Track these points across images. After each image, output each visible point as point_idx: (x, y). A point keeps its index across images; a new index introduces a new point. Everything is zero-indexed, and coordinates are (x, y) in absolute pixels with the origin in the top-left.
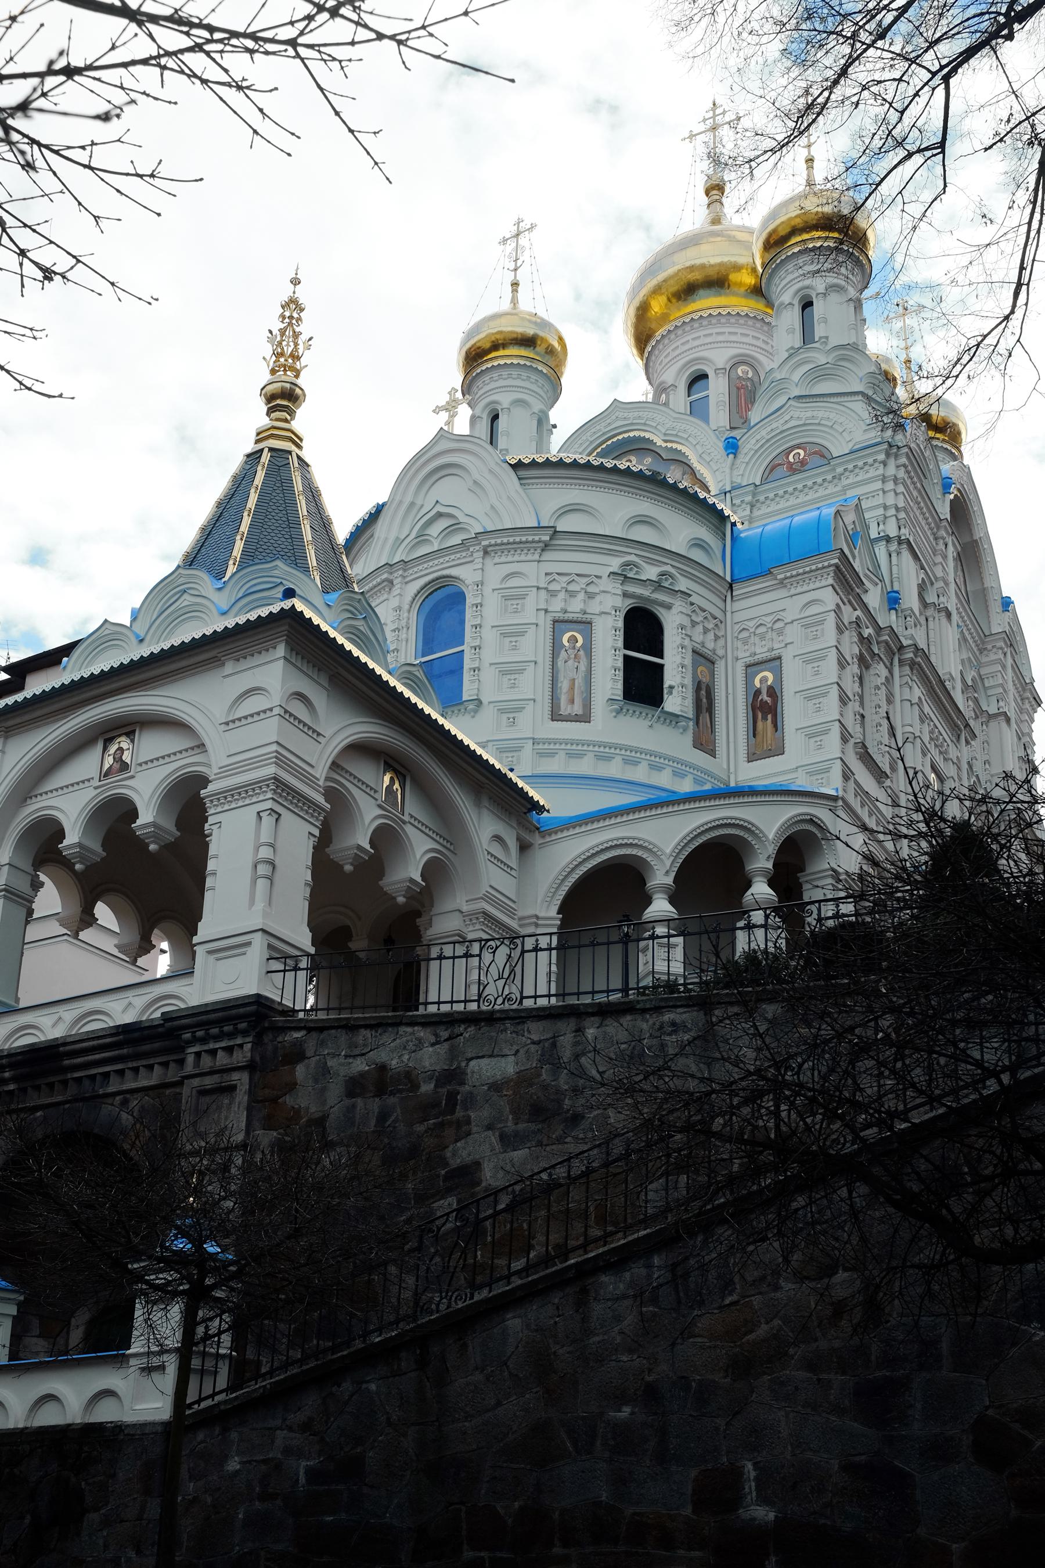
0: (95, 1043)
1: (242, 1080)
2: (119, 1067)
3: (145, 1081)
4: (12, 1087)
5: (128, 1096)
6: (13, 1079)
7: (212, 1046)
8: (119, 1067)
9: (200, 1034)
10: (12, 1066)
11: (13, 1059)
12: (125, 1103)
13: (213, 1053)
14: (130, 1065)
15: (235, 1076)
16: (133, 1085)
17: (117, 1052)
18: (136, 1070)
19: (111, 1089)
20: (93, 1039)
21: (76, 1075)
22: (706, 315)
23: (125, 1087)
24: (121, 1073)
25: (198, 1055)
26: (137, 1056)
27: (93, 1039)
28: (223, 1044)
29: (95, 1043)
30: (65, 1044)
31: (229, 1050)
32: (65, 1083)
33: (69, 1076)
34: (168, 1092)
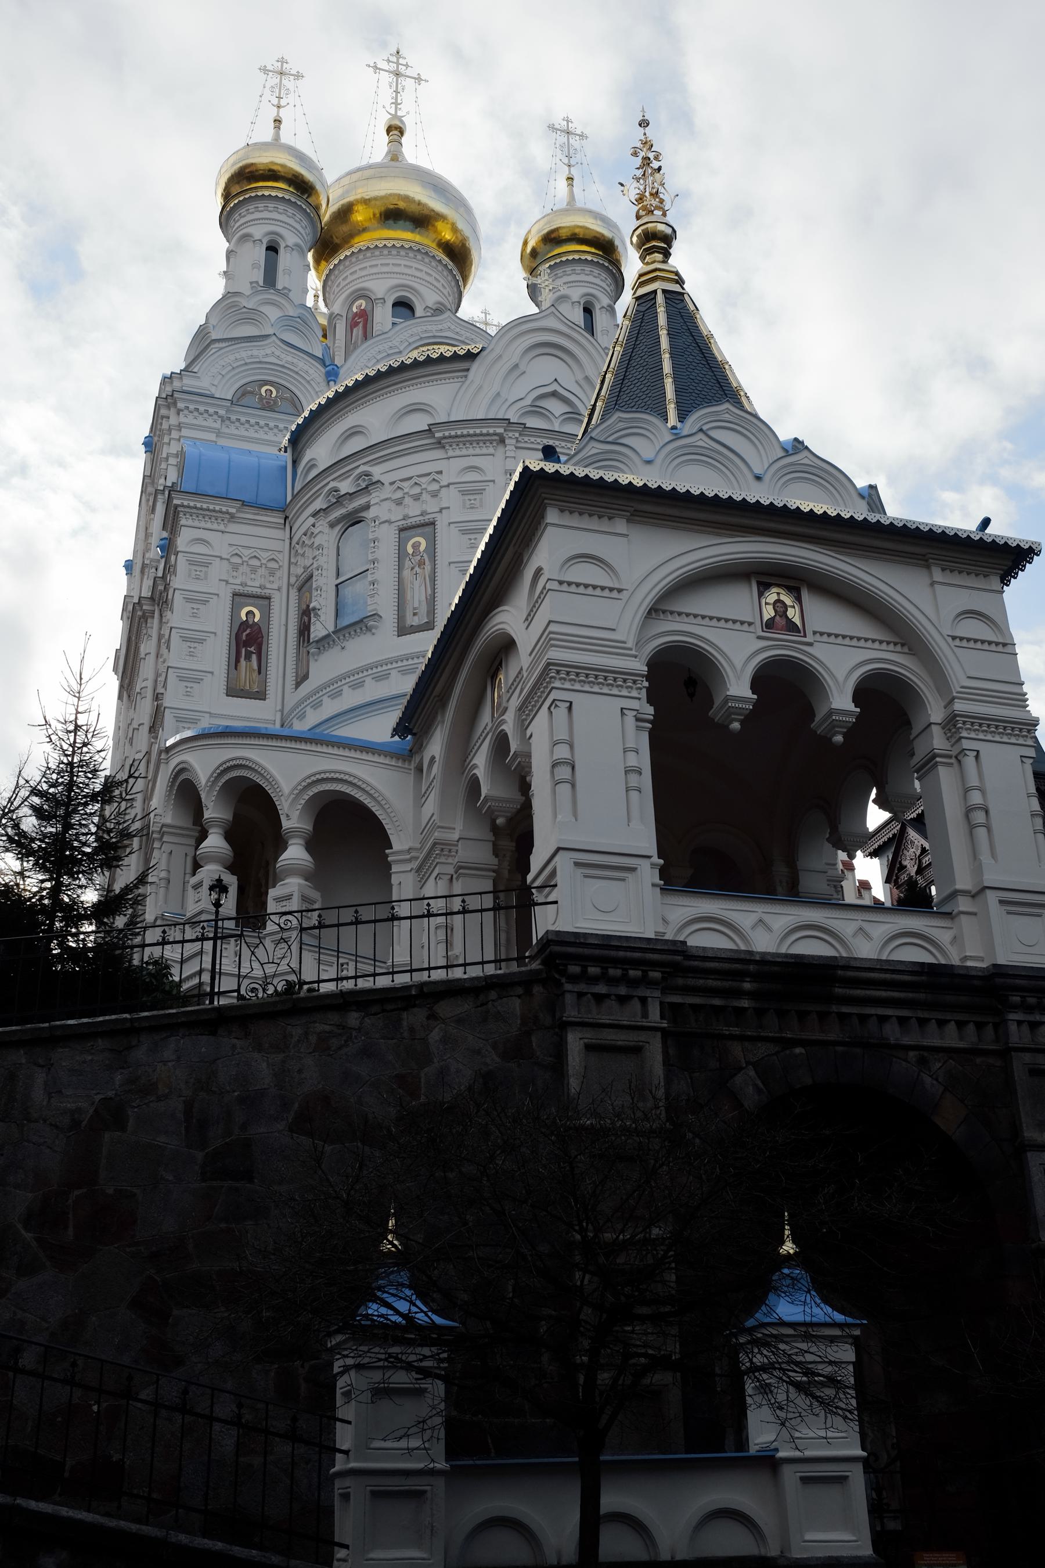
0: (888, 976)
3: (951, 1037)
4: (745, 1003)
5: (926, 1054)
6: (751, 995)
9: (1032, 1000)
12: (922, 1062)
14: (921, 1014)
16: (937, 1042)
17: (910, 995)
18: (922, 1022)
19: (906, 1041)
20: (881, 970)
21: (845, 1009)
22: (407, 246)
23: (926, 1042)
24: (902, 1021)
25: (1019, 1023)
27: (881, 970)
29: (888, 976)
30: (847, 967)
32: (823, 1016)
33: (834, 1008)
34: (978, 1060)
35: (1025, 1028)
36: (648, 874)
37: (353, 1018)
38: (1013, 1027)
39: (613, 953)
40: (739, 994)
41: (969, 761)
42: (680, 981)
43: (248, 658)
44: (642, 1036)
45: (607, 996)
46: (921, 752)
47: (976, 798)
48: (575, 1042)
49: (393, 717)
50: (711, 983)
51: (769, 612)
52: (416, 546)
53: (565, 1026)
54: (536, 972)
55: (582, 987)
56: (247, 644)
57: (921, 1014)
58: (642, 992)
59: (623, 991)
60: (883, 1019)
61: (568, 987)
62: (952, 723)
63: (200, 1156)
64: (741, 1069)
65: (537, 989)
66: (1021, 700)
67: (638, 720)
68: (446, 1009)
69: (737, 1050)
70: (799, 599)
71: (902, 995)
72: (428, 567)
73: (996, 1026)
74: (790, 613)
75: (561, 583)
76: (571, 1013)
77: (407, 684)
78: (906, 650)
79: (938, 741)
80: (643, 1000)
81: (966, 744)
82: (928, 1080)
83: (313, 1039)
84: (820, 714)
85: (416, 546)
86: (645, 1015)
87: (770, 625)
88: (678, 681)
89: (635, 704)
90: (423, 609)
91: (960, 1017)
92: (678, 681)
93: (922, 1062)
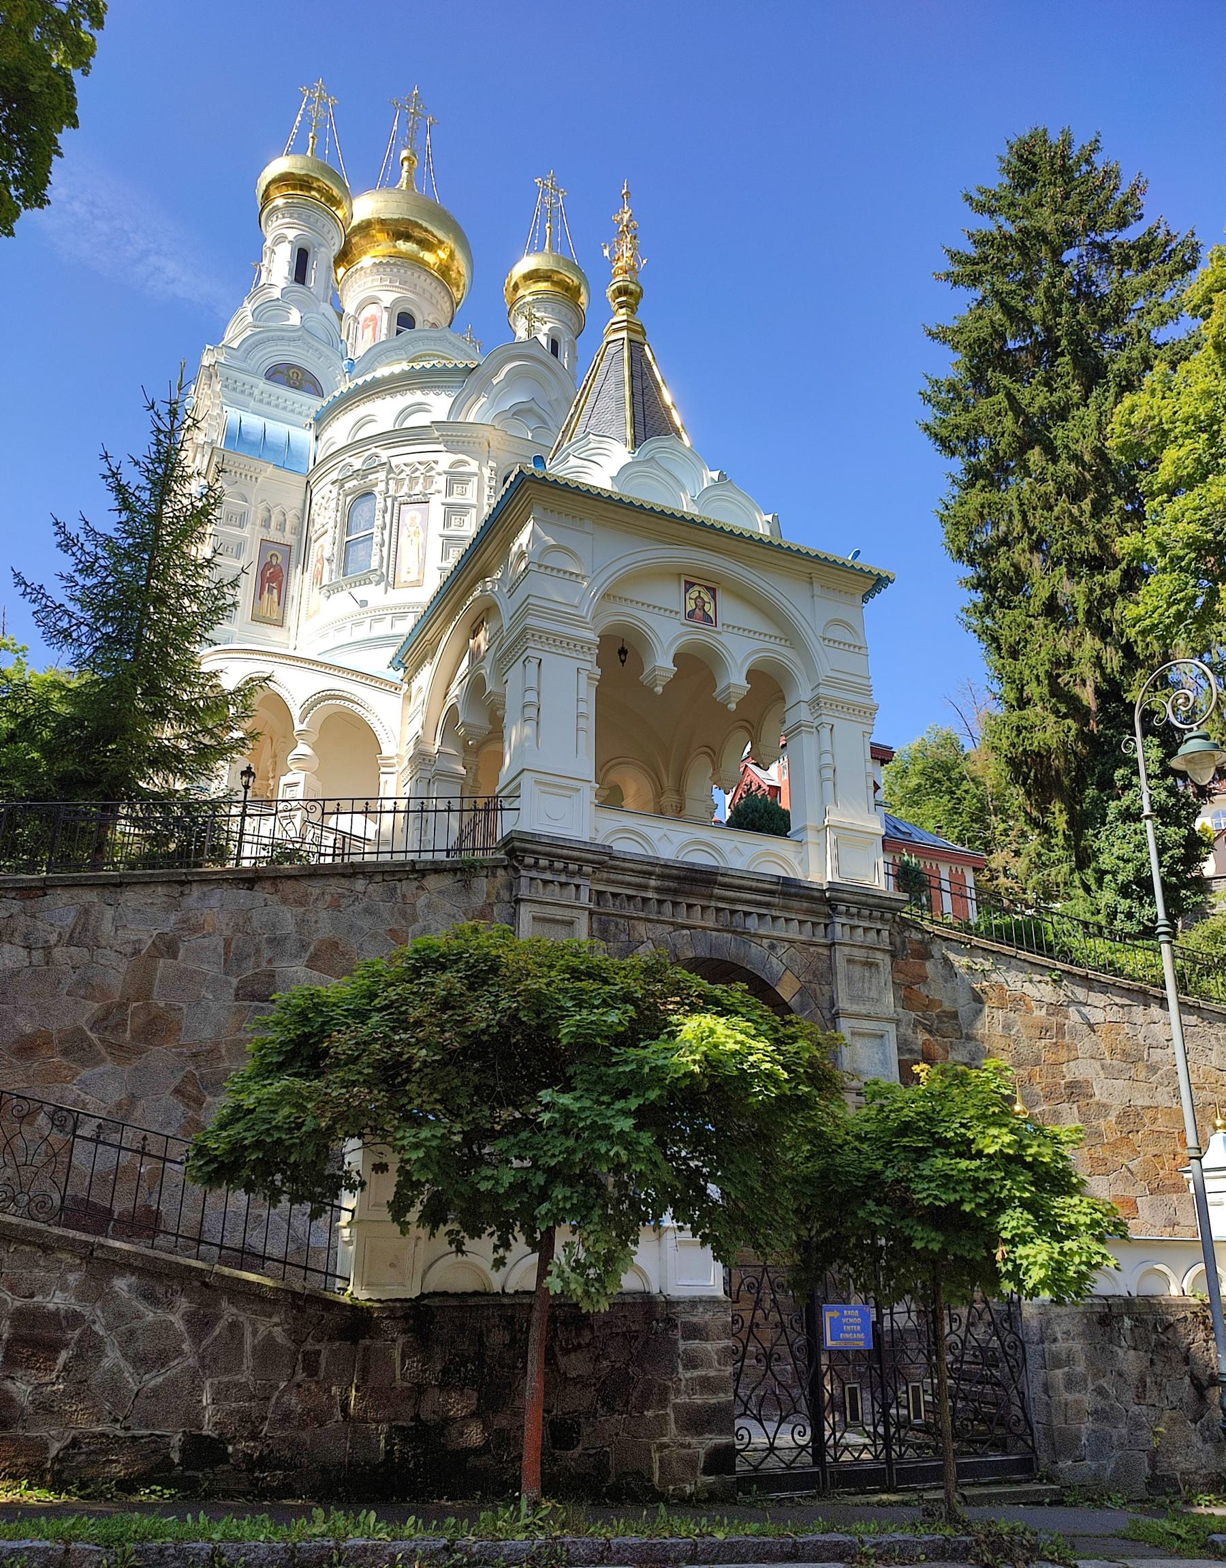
1: (884, 960)
2: (764, 911)
3: (793, 932)
4: (650, 895)
6: (658, 890)
7: (856, 922)
8: (764, 911)
10: (661, 877)
11: (667, 871)
12: (772, 947)
13: (853, 928)
15: (879, 955)
16: (784, 935)
17: (768, 899)
18: (774, 918)
24: (761, 916)
25: (843, 925)
26: (785, 908)
28: (866, 924)
31: (866, 930)
33: (713, 904)
34: (812, 949)
35: (847, 928)
36: (588, 793)
37: (360, 884)
38: (838, 928)
39: (559, 851)
40: (645, 887)
41: (825, 731)
42: (605, 875)
43: (270, 591)
44: (575, 913)
45: (552, 882)
46: (791, 721)
47: (827, 759)
48: (526, 912)
49: (391, 652)
50: (628, 879)
51: (691, 605)
52: (413, 519)
53: (518, 901)
54: (502, 860)
55: (534, 874)
56: (270, 580)
57: (774, 913)
58: (577, 881)
59: (563, 879)
60: (747, 914)
61: (523, 873)
62: (815, 702)
63: (235, 981)
64: (643, 943)
65: (500, 872)
66: (867, 691)
67: (589, 678)
68: (431, 882)
69: (641, 928)
70: (714, 598)
71: (758, 898)
72: (422, 536)
73: (826, 926)
74: (707, 607)
75: (540, 566)
76: (524, 893)
77: (405, 627)
78: (788, 644)
79: (804, 714)
80: (578, 887)
81: (824, 719)
82: (774, 960)
83: (328, 898)
84: (721, 686)
85: (413, 519)
86: (578, 898)
87: (691, 615)
88: (620, 651)
89: (588, 666)
90: (415, 570)
91: (801, 917)
92: (620, 651)
93: (772, 947)
